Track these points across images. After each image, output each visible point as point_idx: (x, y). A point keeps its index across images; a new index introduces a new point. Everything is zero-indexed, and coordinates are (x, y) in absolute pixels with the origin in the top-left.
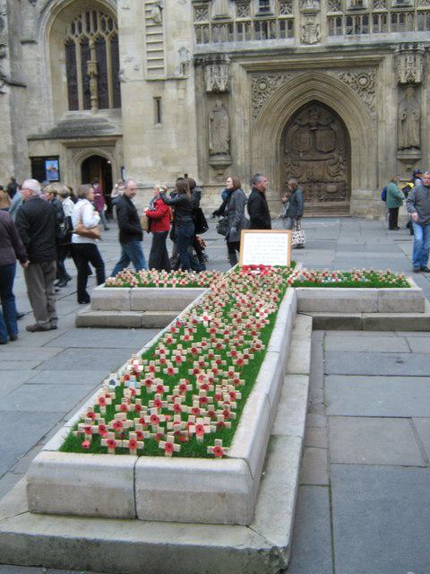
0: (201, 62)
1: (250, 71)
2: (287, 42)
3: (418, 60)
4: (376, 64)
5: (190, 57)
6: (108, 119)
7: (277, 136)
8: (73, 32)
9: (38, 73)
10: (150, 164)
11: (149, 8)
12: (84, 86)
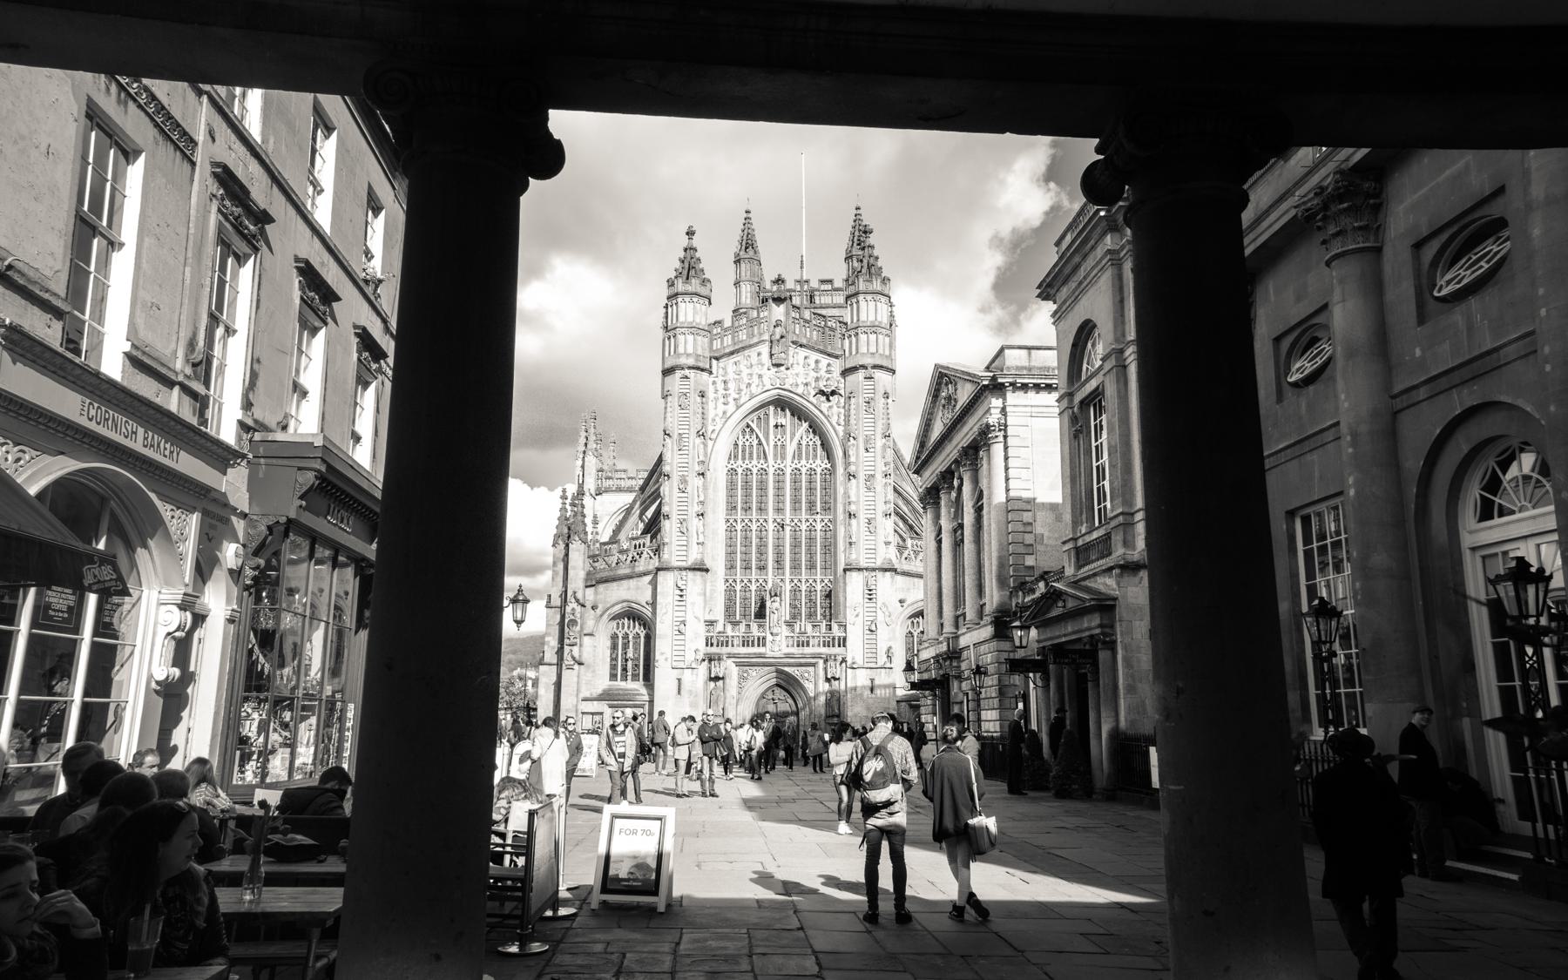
2: (761, 650)
5: (700, 656)
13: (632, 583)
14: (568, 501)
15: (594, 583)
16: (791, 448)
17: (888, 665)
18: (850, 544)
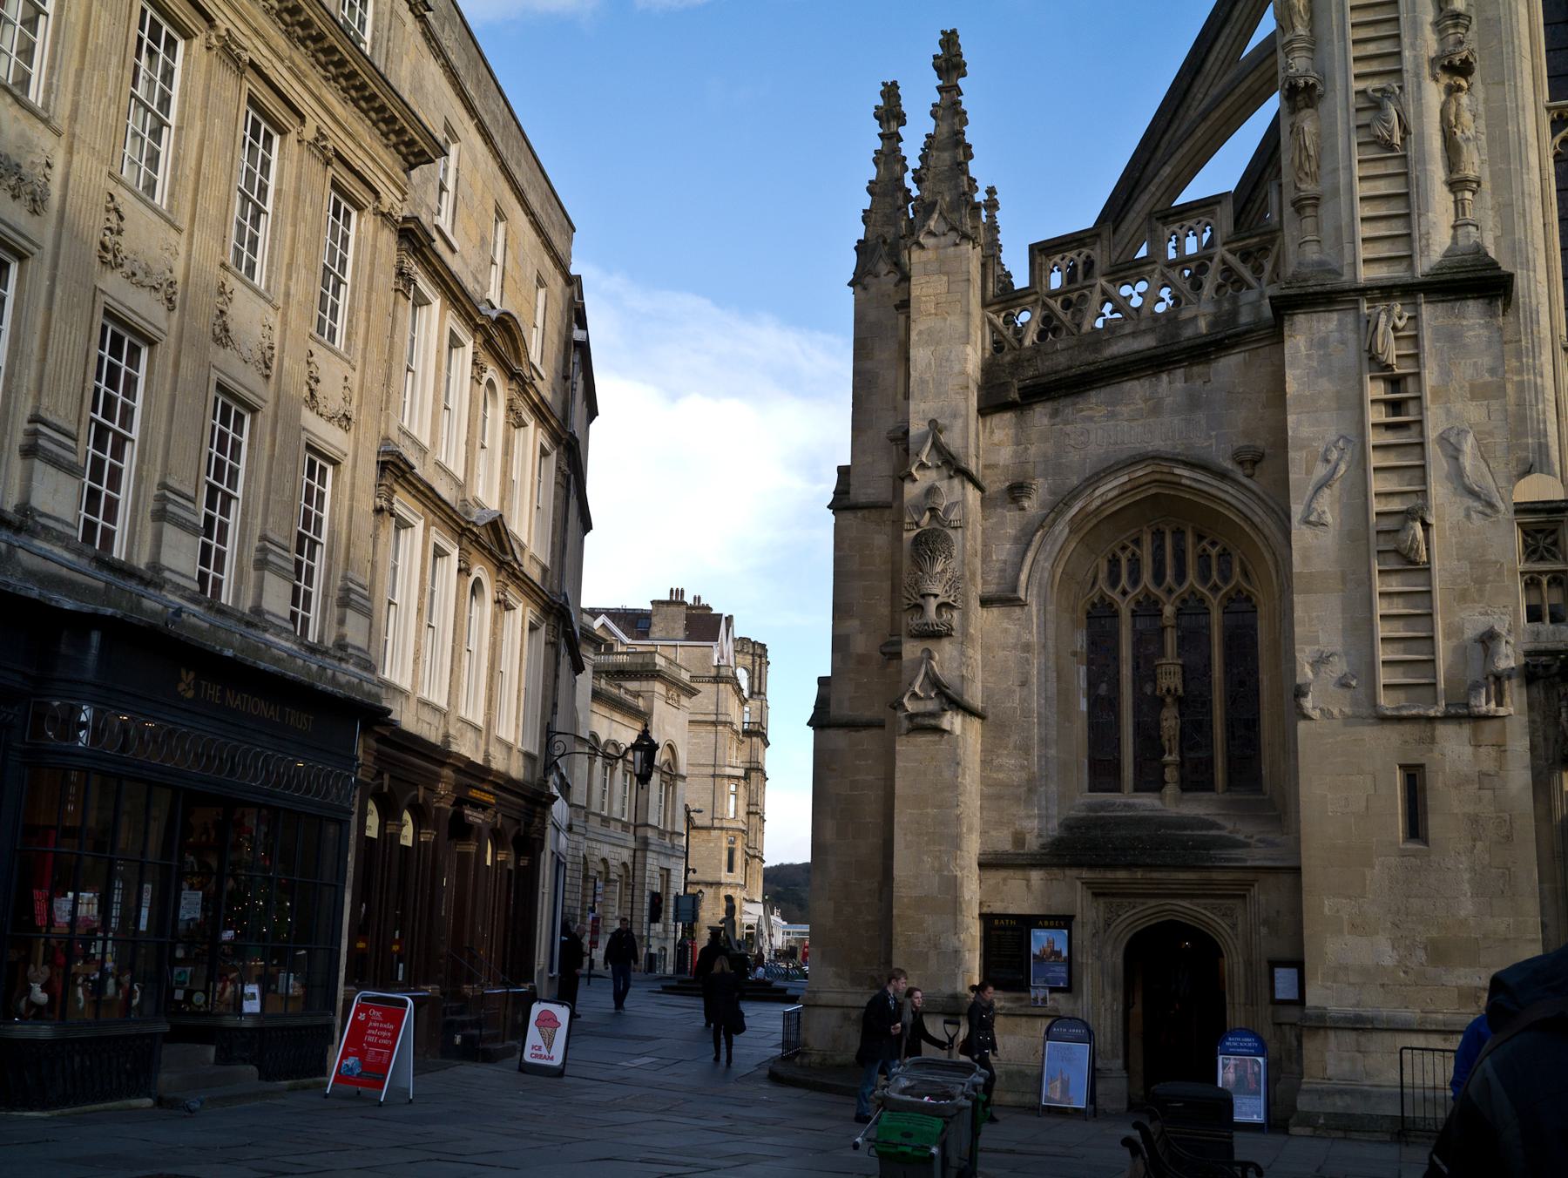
6: (1219, 820)
8: (1114, 580)
9: (1023, 684)
10: (1389, 958)
12: (1138, 727)
13: (1171, 386)
14: (912, 148)
15: (1014, 395)
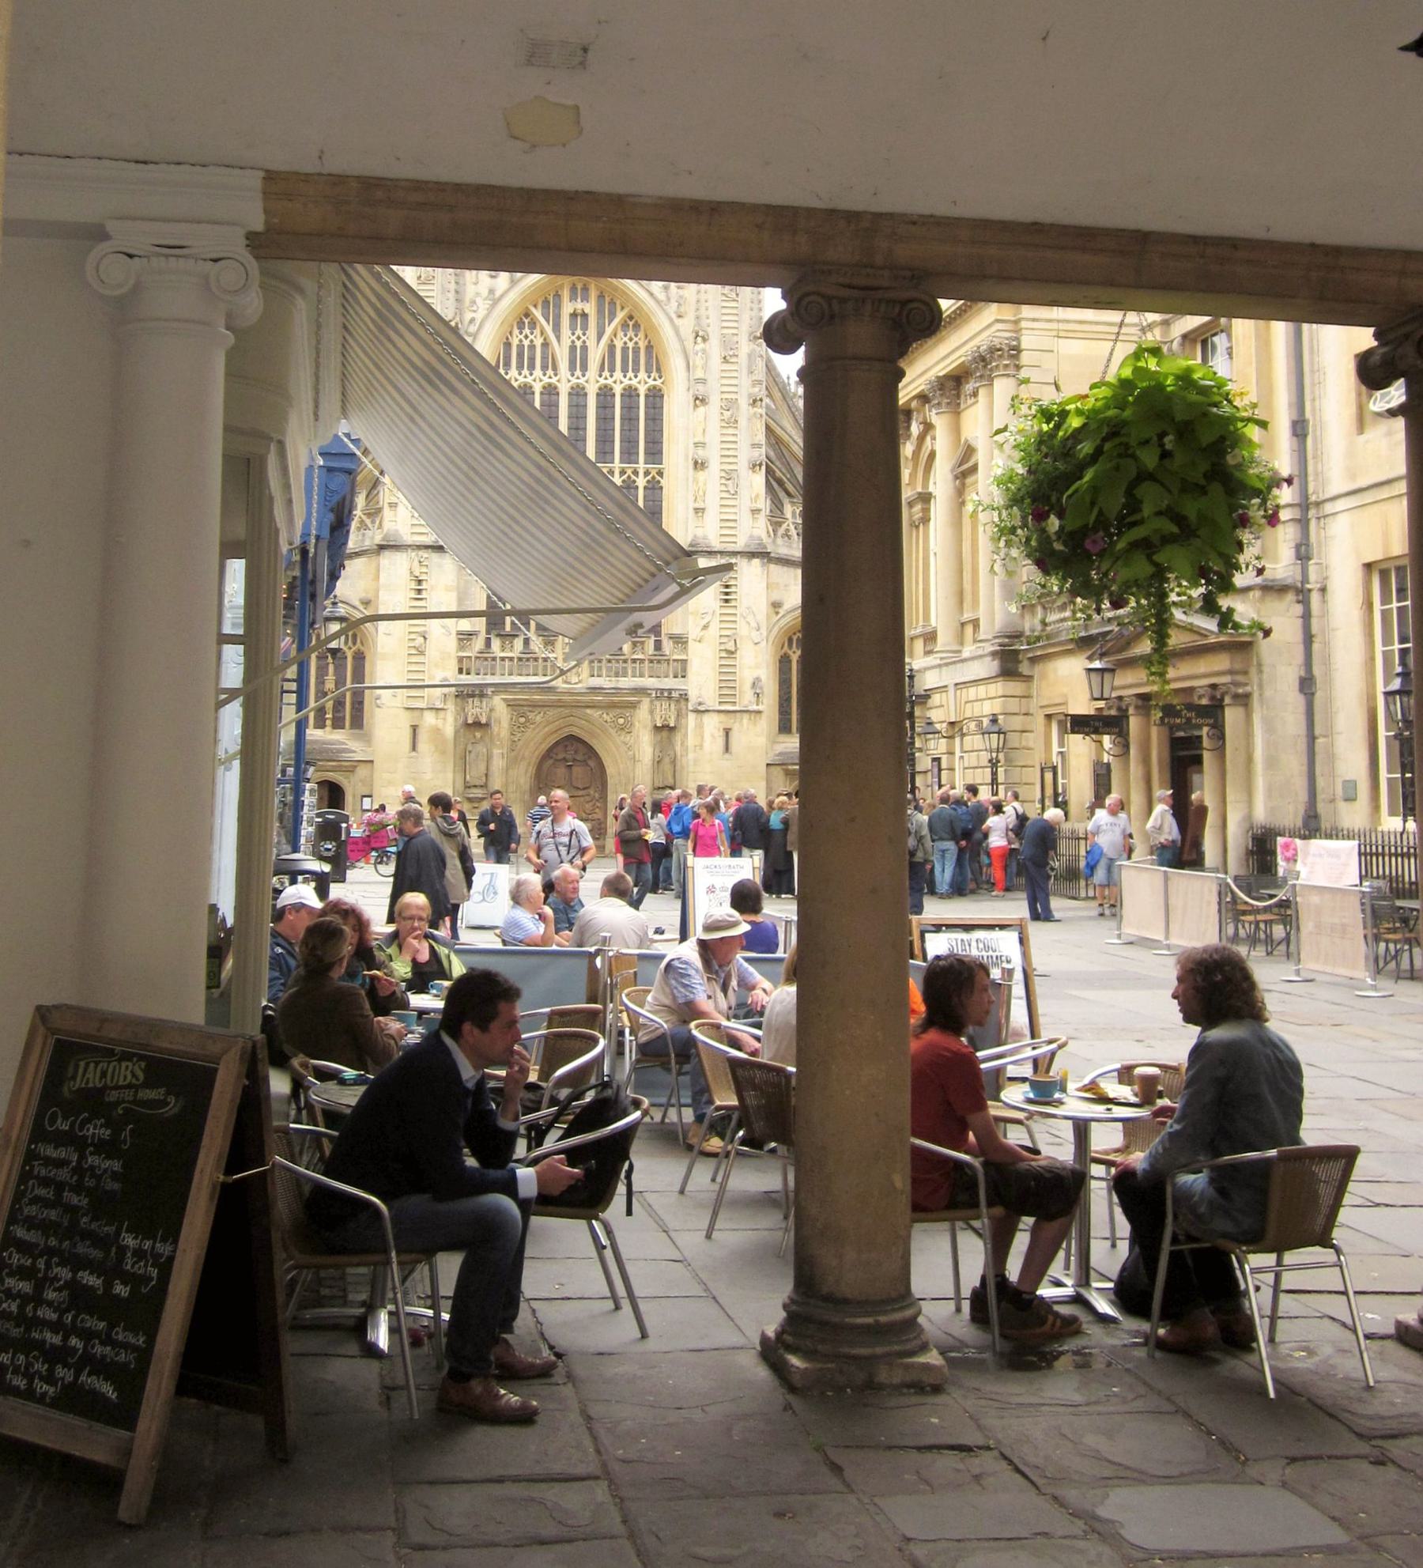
0: (465, 694)
1: (510, 704)
3: (673, 706)
4: (634, 706)
7: (532, 770)
11: (413, 636)
16: (596, 355)
17: (755, 707)
18: (697, 510)
